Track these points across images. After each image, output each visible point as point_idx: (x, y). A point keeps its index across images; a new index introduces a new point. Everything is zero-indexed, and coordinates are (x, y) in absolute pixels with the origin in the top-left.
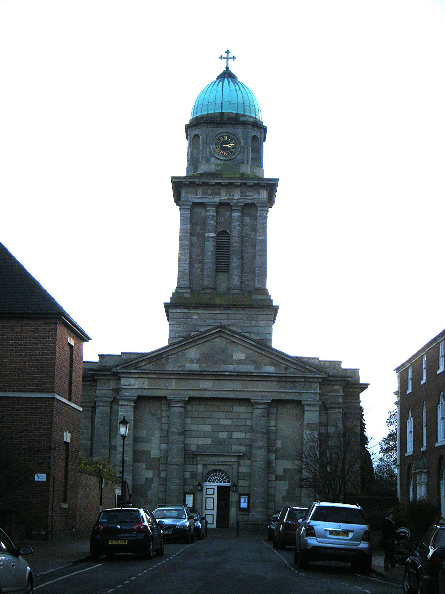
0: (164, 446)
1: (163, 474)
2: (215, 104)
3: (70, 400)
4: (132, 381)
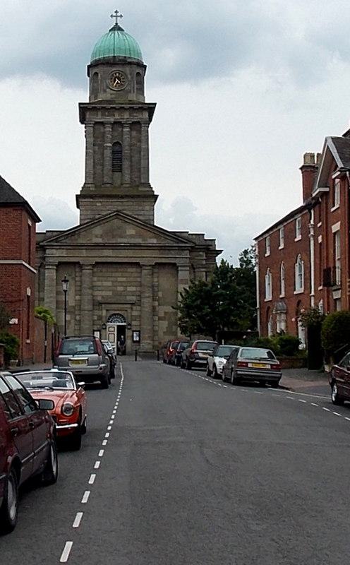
0: (78, 297)
3: (29, 264)
4: (54, 251)
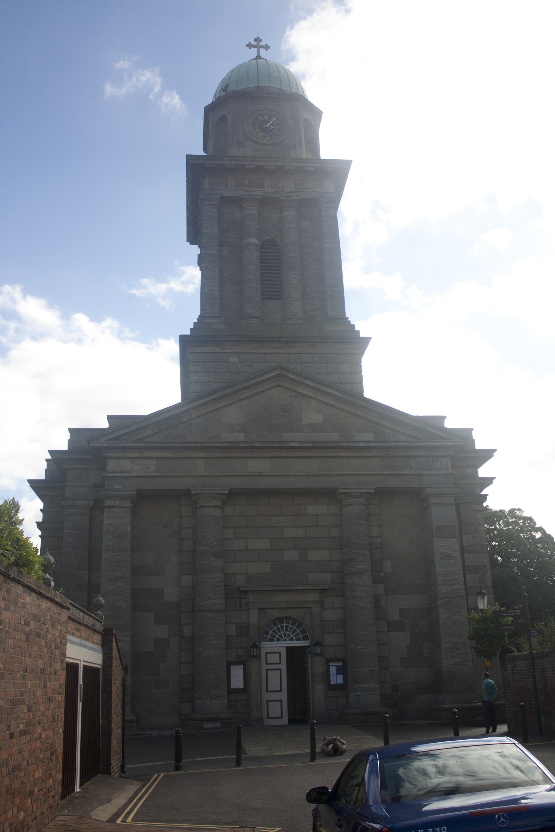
0: (186, 580)
1: (187, 631)
2: (248, 77)
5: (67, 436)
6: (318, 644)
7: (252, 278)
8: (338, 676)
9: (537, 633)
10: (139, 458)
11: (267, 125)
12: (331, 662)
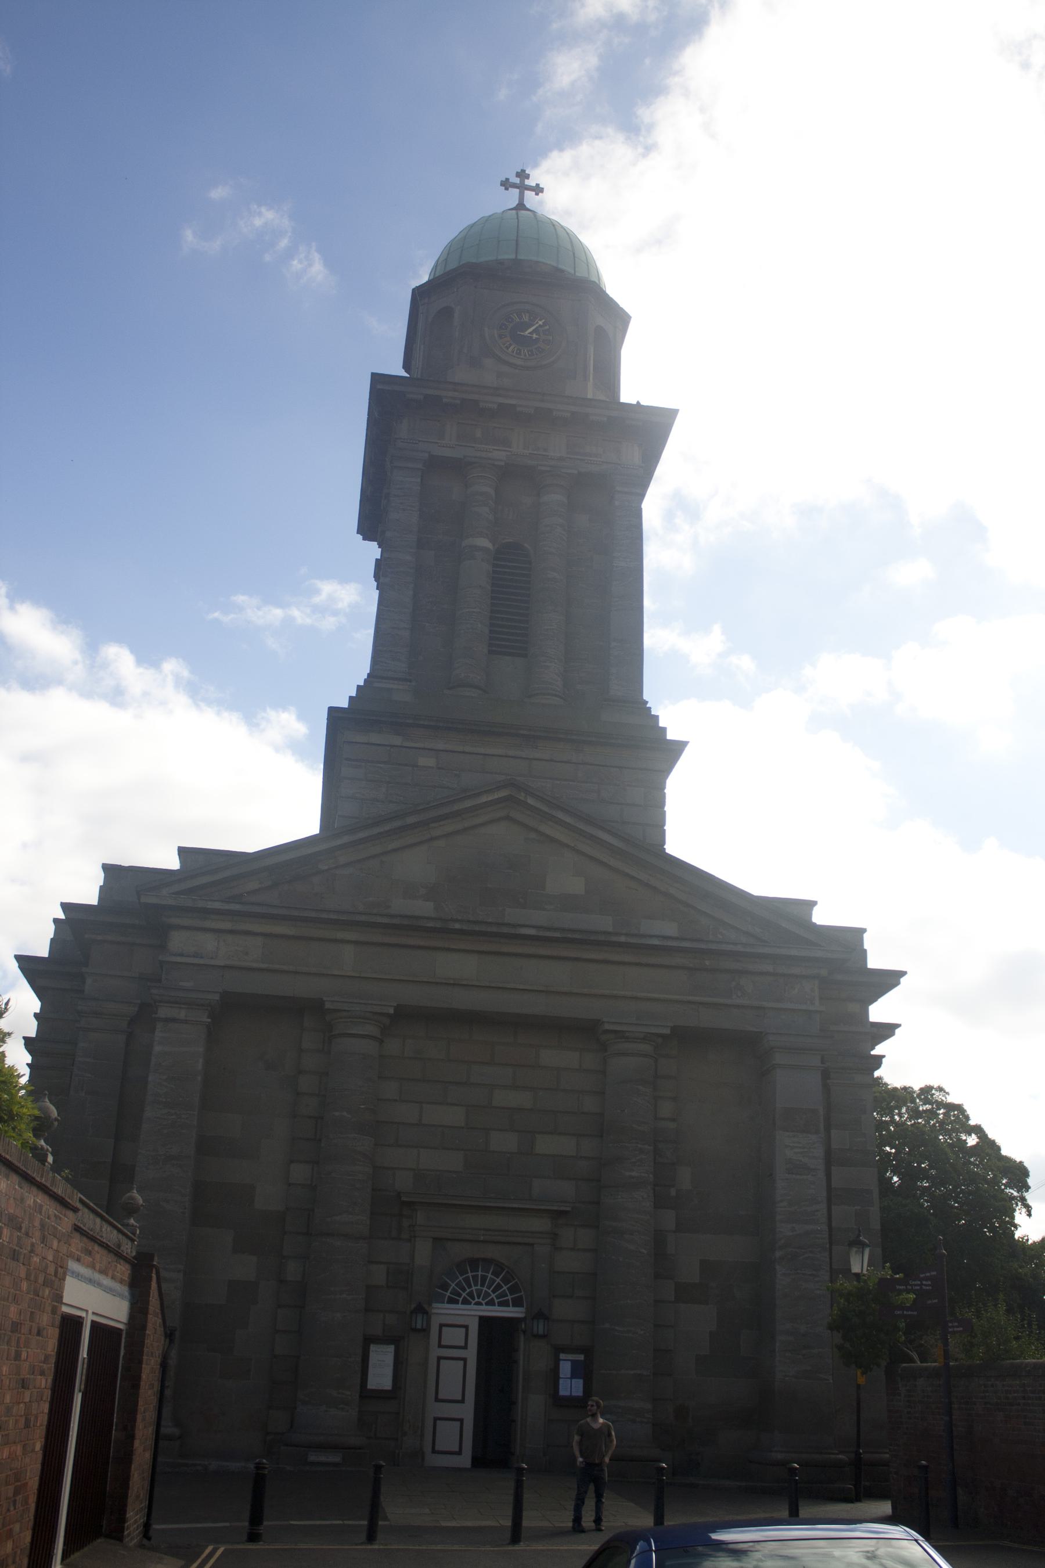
5: (100, 878)
6: (540, 1315)
7: (474, 612)
8: (573, 1380)
9: (961, 1329)
10: (232, 932)
11: (527, 333)
12: (563, 1352)
